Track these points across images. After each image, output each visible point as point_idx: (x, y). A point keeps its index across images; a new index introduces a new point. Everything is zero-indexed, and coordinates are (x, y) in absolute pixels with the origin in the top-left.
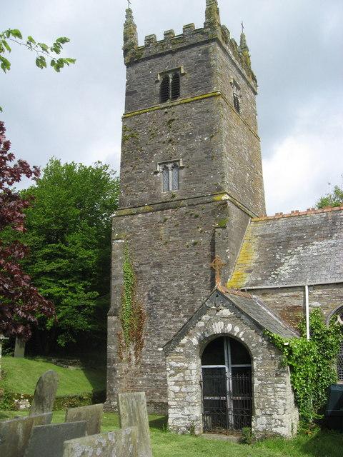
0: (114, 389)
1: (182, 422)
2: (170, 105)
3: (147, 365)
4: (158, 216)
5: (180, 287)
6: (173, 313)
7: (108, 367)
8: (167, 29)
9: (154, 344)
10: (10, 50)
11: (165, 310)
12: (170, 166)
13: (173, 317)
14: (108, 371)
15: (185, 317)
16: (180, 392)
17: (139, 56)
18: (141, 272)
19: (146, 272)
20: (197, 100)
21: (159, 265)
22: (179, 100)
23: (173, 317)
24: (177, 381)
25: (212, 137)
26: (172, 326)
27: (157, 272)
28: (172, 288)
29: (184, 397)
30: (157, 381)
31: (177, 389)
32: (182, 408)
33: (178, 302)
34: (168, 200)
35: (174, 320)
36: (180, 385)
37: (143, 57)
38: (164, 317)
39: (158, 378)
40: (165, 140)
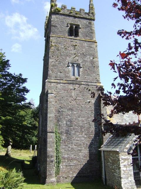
0: (52, 172)
1: (128, 185)
2: (73, 38)
3: (65, 158)
4: (71, 87)
5: (83, 121)
6: (79, 133)
7: (48, 160)
8: (73, 7)
9: (69, 147)
10: (123, 16)
11: (75, 131)
12: (75, 65)
13: (79, 135)
14: (48, 162)
15: (85, 135)
16: (126, 170)
17: (59, 11)
18: (62, 111)
19: (65, 112)
20: (87, 41)
21: (71, 109)
22: (78, 38)
23: (79, 135)
24: (125, 165)
25: (94, 58)
26: (79, 139)
27: (70, 112)
28: (79, 121)
29: (128, 173)
30: (71, 166)
31: (125, 169)
32: (128, 178)
33: (82, 127)
34: (74, 80)
35: (80, 136)
36: (126, 167)
37: (61, 13)
38: (75, 134)
39: (72, 164)
40: (73, 53)
